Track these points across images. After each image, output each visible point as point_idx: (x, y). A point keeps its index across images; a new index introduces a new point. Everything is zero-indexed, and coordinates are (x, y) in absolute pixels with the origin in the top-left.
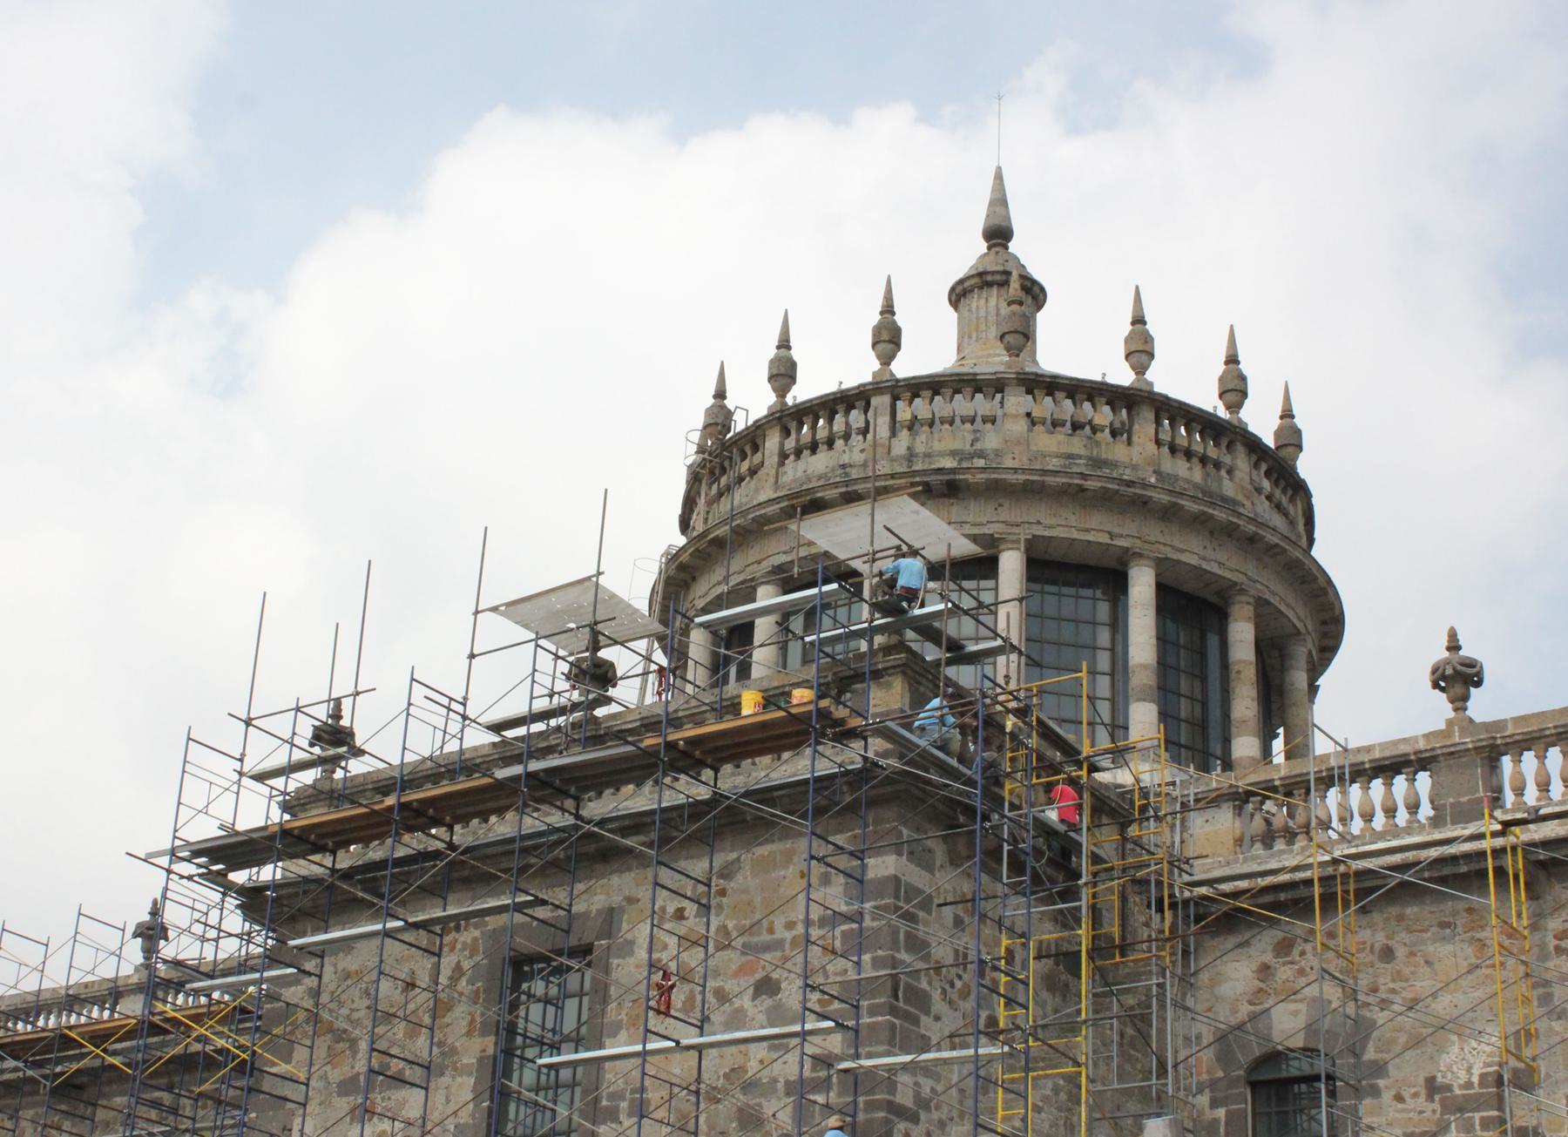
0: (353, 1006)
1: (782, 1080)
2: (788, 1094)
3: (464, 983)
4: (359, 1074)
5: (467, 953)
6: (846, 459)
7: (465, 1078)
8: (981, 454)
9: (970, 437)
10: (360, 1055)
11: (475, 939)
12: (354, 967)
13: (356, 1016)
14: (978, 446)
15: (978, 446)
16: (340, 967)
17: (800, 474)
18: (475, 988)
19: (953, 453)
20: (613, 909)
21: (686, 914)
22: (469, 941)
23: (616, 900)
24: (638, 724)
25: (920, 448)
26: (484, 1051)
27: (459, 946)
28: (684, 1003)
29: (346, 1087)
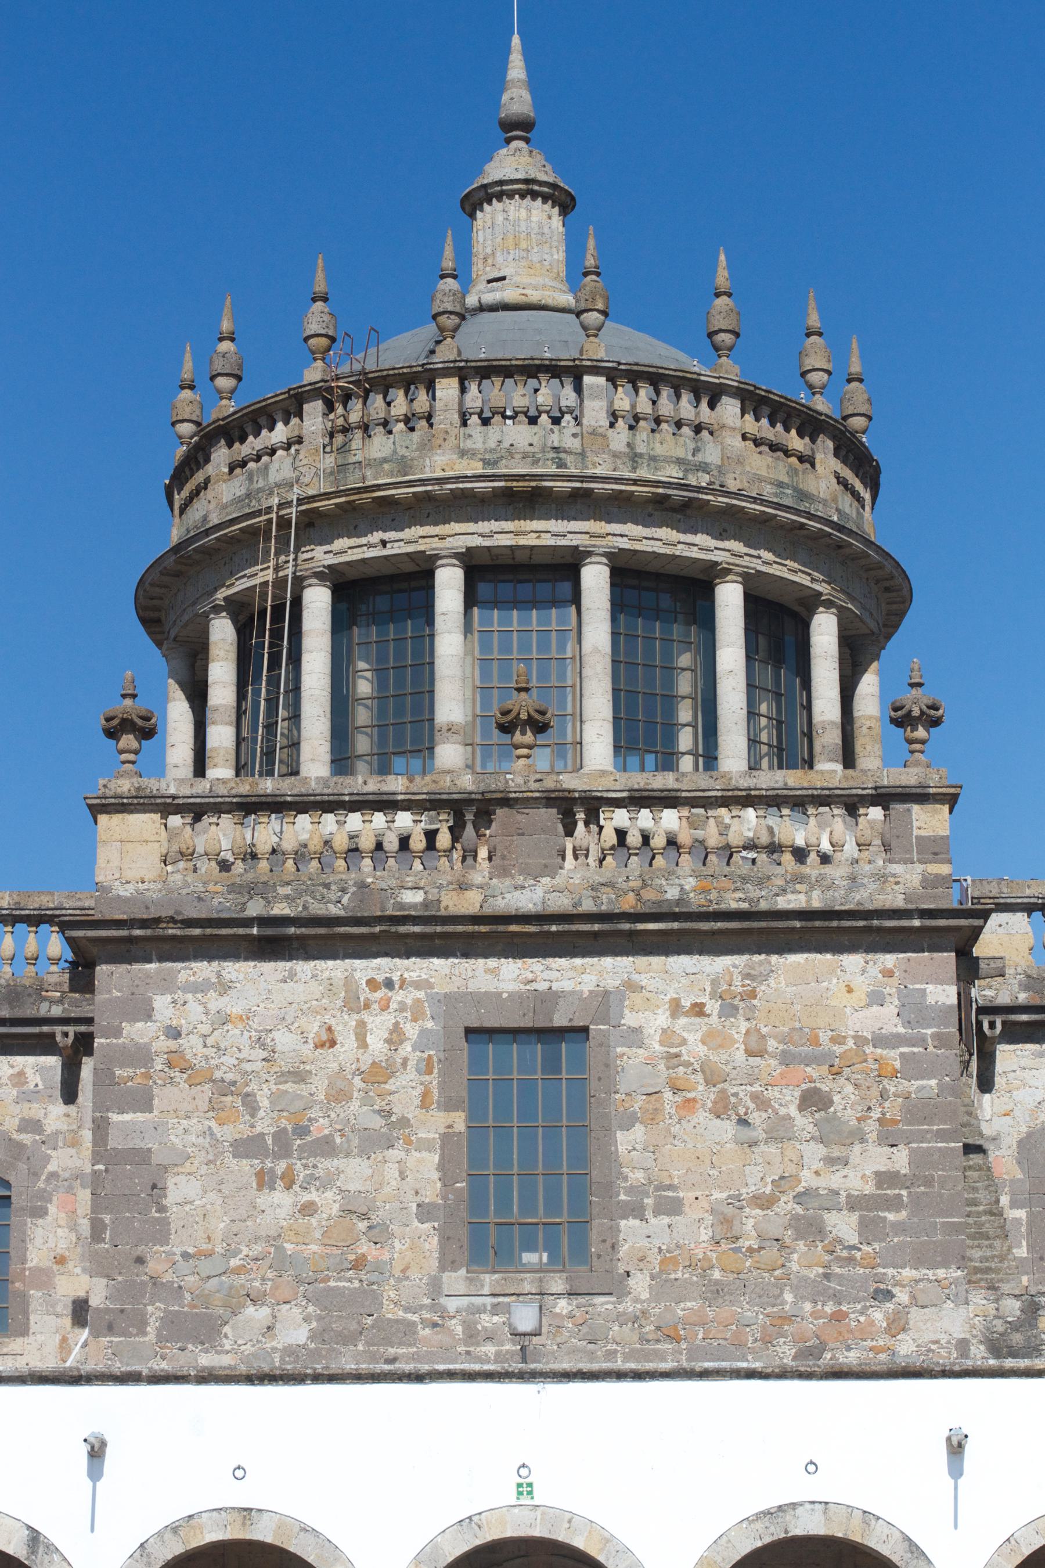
0: (241, 1056)
1: (843, 1194)
2: (852, 1209)
3: (409, 1049)
4: (262, 1135)
5: (408, 1014)
6: (555, 439)
7: (425, 1154)
8: (704, 468)
9: (691, 445)
10: (261, 1113)
11: (418, 1000)
12: (237, 1010)
13: (248, 1067)
14: (699, 457)
15: (699, 457)
16: (213, 1006)
17: (492, 444)
18: (425, 1055)
19: (679, 462)
20: (606, 993)
21: (708, 1009)
22: (409, 1002)
23: (612, 983)
24: (625, 794)
25: (641, 448)
26: (450, 1127)
27: (393, 1006)
28: (715, 1103)
29: (246, 1147)
